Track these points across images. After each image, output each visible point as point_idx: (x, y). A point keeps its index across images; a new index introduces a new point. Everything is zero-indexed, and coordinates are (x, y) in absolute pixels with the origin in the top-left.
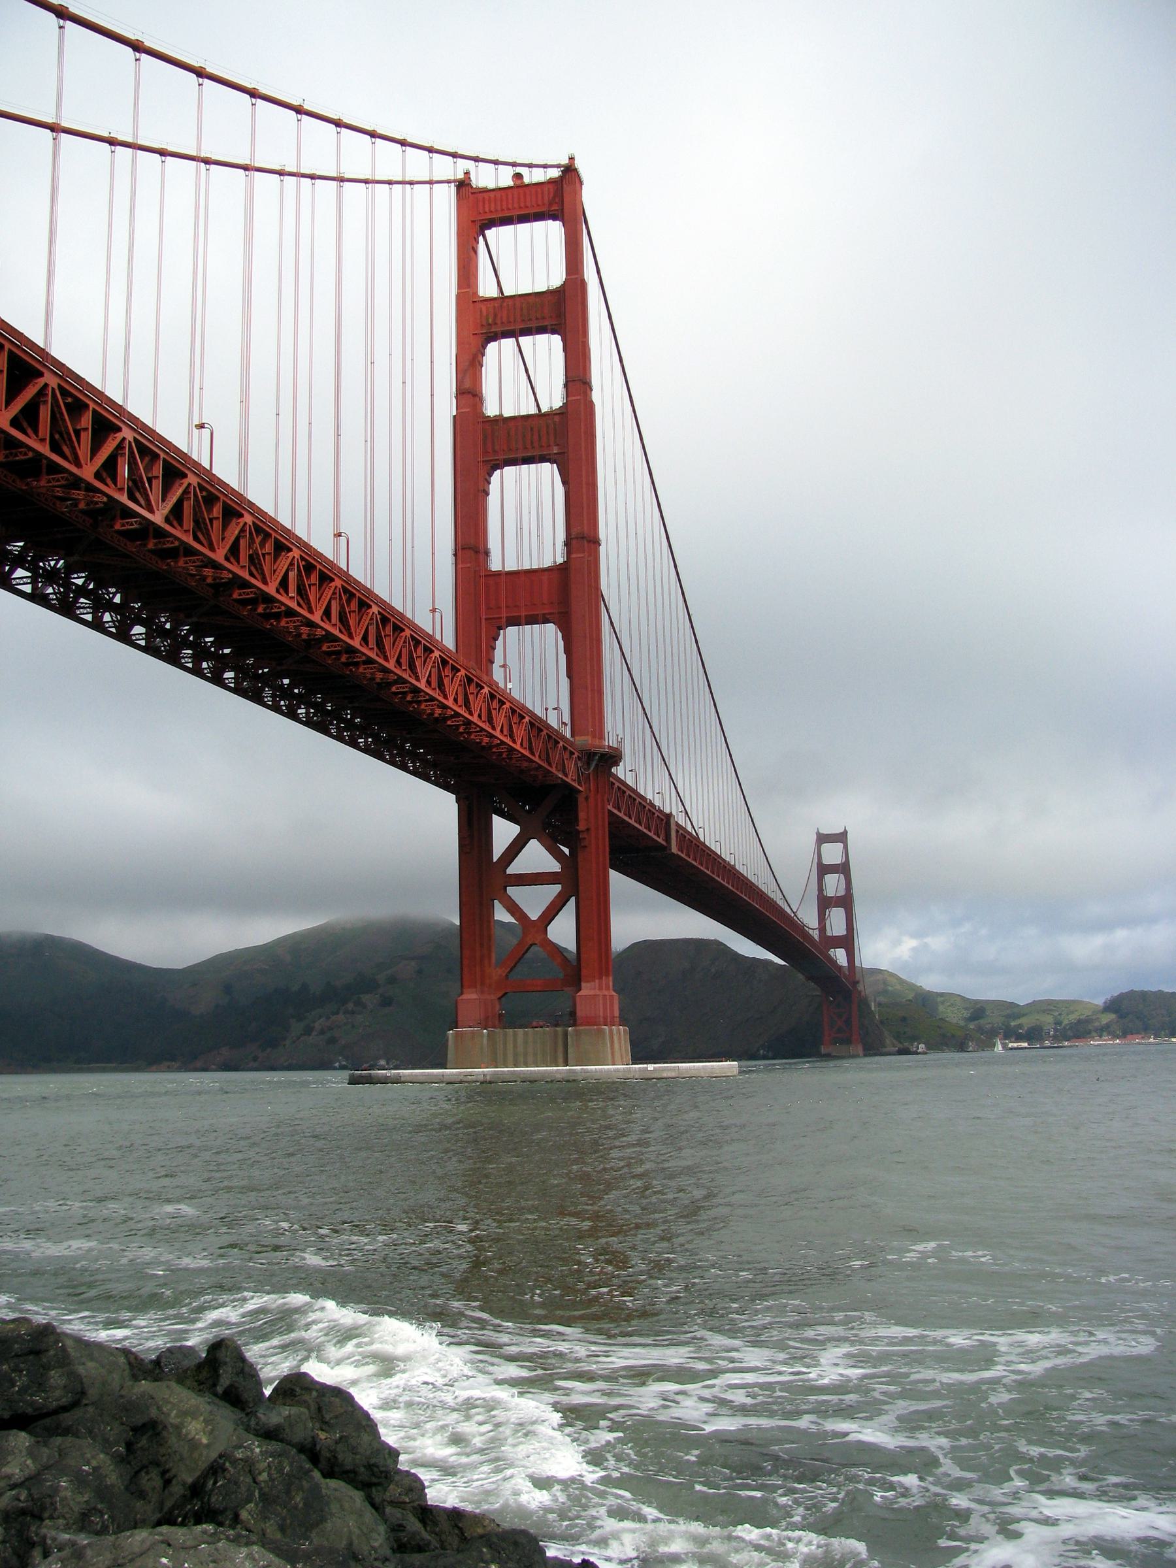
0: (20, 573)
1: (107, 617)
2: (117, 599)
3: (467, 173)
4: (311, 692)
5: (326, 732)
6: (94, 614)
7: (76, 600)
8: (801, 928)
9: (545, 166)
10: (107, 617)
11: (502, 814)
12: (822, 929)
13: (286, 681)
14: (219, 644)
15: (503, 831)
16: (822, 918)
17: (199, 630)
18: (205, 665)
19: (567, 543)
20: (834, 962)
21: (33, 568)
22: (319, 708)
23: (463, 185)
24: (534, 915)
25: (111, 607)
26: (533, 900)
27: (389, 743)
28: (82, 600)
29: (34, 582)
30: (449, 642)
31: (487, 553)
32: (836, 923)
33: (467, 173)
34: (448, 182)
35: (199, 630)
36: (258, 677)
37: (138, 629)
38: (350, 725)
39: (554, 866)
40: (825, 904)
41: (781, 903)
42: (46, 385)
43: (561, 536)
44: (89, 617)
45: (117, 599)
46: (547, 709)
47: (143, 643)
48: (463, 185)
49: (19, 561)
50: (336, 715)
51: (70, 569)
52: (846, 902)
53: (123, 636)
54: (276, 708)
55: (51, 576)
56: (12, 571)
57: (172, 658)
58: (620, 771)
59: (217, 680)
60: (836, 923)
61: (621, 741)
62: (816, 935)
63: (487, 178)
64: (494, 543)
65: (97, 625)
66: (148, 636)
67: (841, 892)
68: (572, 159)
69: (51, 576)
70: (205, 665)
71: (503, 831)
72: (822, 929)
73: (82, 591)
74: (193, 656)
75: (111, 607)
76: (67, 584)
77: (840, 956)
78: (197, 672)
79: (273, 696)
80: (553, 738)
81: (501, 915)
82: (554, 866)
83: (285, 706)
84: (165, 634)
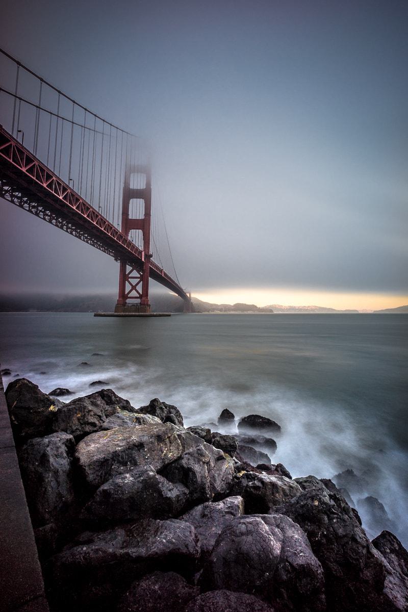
0: (26, 205)
1: (47, 217)
2: (49, 214)
4: (84, 234)
6: (44, 216)
7: (39, 213)
10: (47, 217)
11: (128, 265)
13: (86, 235)
15: (129, 268)
17: (68, 223)
19: (145, 215)
21: (29, 204)
22: (93, 241)
25: (47, 215)
26: (134, 282)
29: (29, 208)
31: (128, 215)
35: (68, 223)
36: (80, 234)
37: (54, 221)
42: (35, 164)
43: (144, 213)
44: (42, 217)
45: (49, 214)
49: (26, 202)
51: (38, 206)
55: (34, 207)
56: (23, 205)
59: (71, 233)
64: (130, 213)
69: (34, 207)
73: (41, 211)
75: (47, 215)
76: (38, 209)
84: (60, 223)
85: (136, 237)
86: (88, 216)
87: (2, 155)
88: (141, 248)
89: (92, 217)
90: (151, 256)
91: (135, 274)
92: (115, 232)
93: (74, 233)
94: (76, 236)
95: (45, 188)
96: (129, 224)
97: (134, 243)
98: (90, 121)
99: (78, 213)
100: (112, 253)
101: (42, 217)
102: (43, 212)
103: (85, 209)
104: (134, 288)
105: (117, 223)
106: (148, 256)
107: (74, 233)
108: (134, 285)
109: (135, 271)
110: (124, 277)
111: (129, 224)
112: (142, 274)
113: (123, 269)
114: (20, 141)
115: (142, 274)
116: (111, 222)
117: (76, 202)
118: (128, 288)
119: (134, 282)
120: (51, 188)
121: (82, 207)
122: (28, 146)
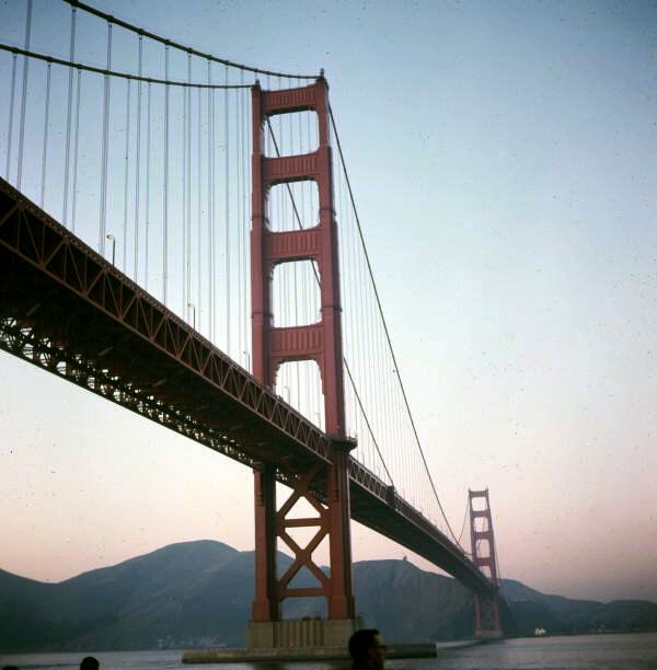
1: (42, 357)
3: (258, 82)
5: (176, 429)
7: (24, 345)
8: (461, 554)
9: (307, 77)
10: (42, 357)
11: (281, 481)
12: (474, 553)
13: (152, 398)
14: (111, 374)
16: (474, 549)
18: (102, 387)
20: (482, 574)
22: (173, 415)
23: (256, 88)
24: (303, 545)
26: (303, 536)
27: (213, 436)
28: (28, 345)
30: (251, 373)
32: (484, 552)
33: (258, 82)
34: (248, 86)
36: (134, 395)
37: (62, 365)
38: (191, 425)
39: (315, 514)
40: (475, 536)
41: (450, 537)
44: (31, 357)
47: (64, 373)
48: (256, 88)
50: (182, 419)
52: (489, 535)
53: (52, 369)
54: (145, 414)
57: (83, 383)
58: (353, 453)
59: (110, 396)
60: (484, 552)
61: (356, 436)
62: (470, 558)
63: (270, 85)
65: (36, 362)
66: (67, 369)
67: (486, 529)
68: (322, 72)
70: (102, 387)
71: (283, 493)
72: (474, 553)
73: (28, 340)
74: (96, 382)
75: (44, 349)
77: (486, 571)
78: (97, 391)
79: (144, 407)
80: (316, 432)
81: (281, 546)
82: (315, 514)
85: (299, 387)
86: (184, 357)
87: (4, 243)
89: (141, 320)
90: (353, 444)
91: (304, 509)
92: (238, 374)
93: (117, 393)
94: (122, 403)
95: (42, 275)
96: (273, 345)
97: (294, 405)
98: (155, 59)
99: (208, 383)
100: (231, 445)
101: (31, 357)
102: (31, 342)
103: (117, 296)
105: (235, 343)
106: (343, 445)
107: (117, 393)
108: (303, 545)
109: (303, 503)
110: (271, 522)
111: (273, 345)
112: (326, 507)
113: (265, 495)
115: (326, 507)
116: (296, 408)
117: (124, 304)
119: (303, 536)
120: (58, 272)
121: (140, 313)
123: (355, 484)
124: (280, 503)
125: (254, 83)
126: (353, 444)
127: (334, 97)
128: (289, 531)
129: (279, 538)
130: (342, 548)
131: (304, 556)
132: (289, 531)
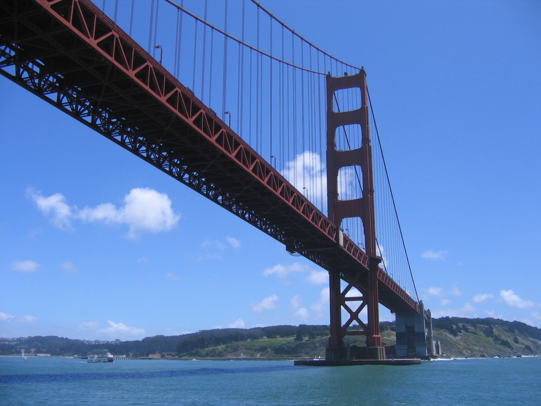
26: (354, 306)
39: (360, 295)
46: (359, 244)
58: (381, 265)
82: (360, 295)
83: (240, 213)
88: (362, 248)
90: (379, 260)
91: (354, 292)
104: (354, 316)
114: (158, 59)
118: (345, 317)
122: (168, 66)
123: (380, 280)
124: (342, 290)
125: (327, 73)
126: (379, 260)
127: (369, 81)
128: (347, 303)
129: (342, 307)
130: (373, 314)
131: (354, 316)
132: (347, 303)
